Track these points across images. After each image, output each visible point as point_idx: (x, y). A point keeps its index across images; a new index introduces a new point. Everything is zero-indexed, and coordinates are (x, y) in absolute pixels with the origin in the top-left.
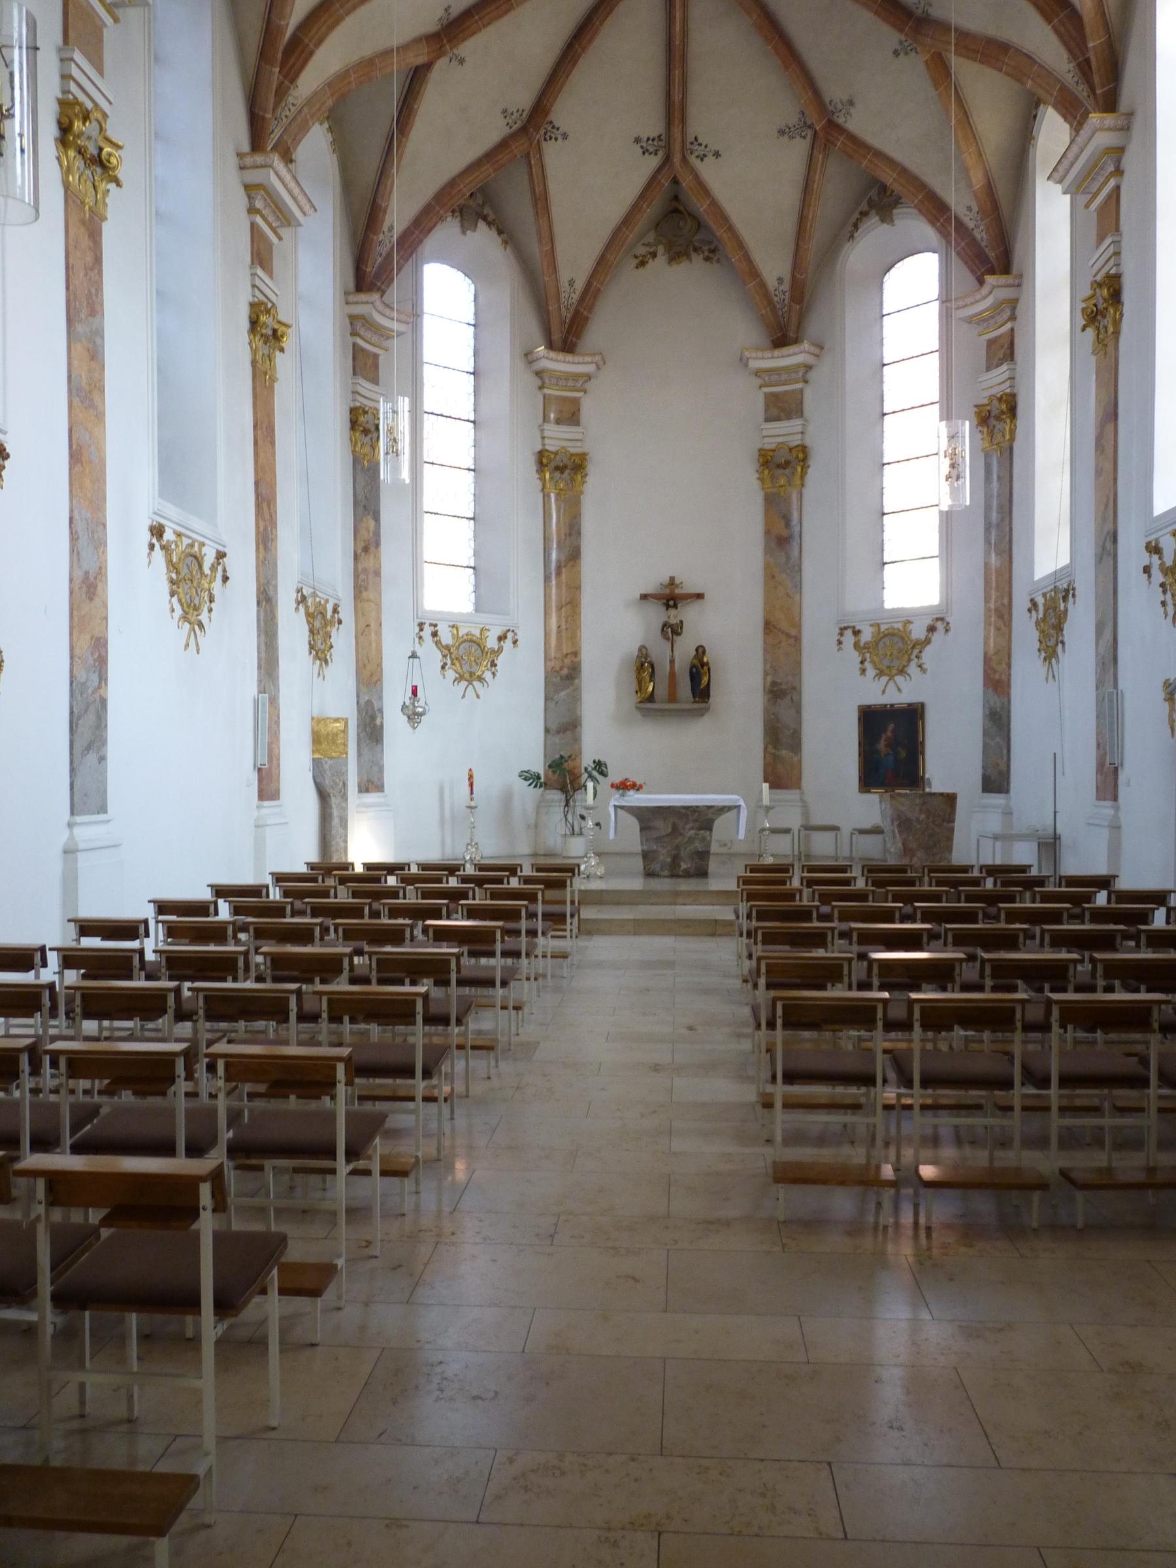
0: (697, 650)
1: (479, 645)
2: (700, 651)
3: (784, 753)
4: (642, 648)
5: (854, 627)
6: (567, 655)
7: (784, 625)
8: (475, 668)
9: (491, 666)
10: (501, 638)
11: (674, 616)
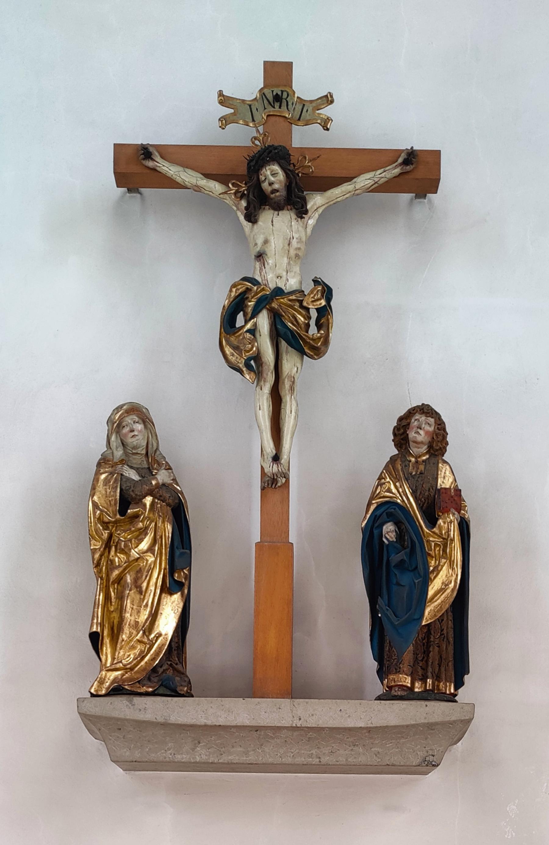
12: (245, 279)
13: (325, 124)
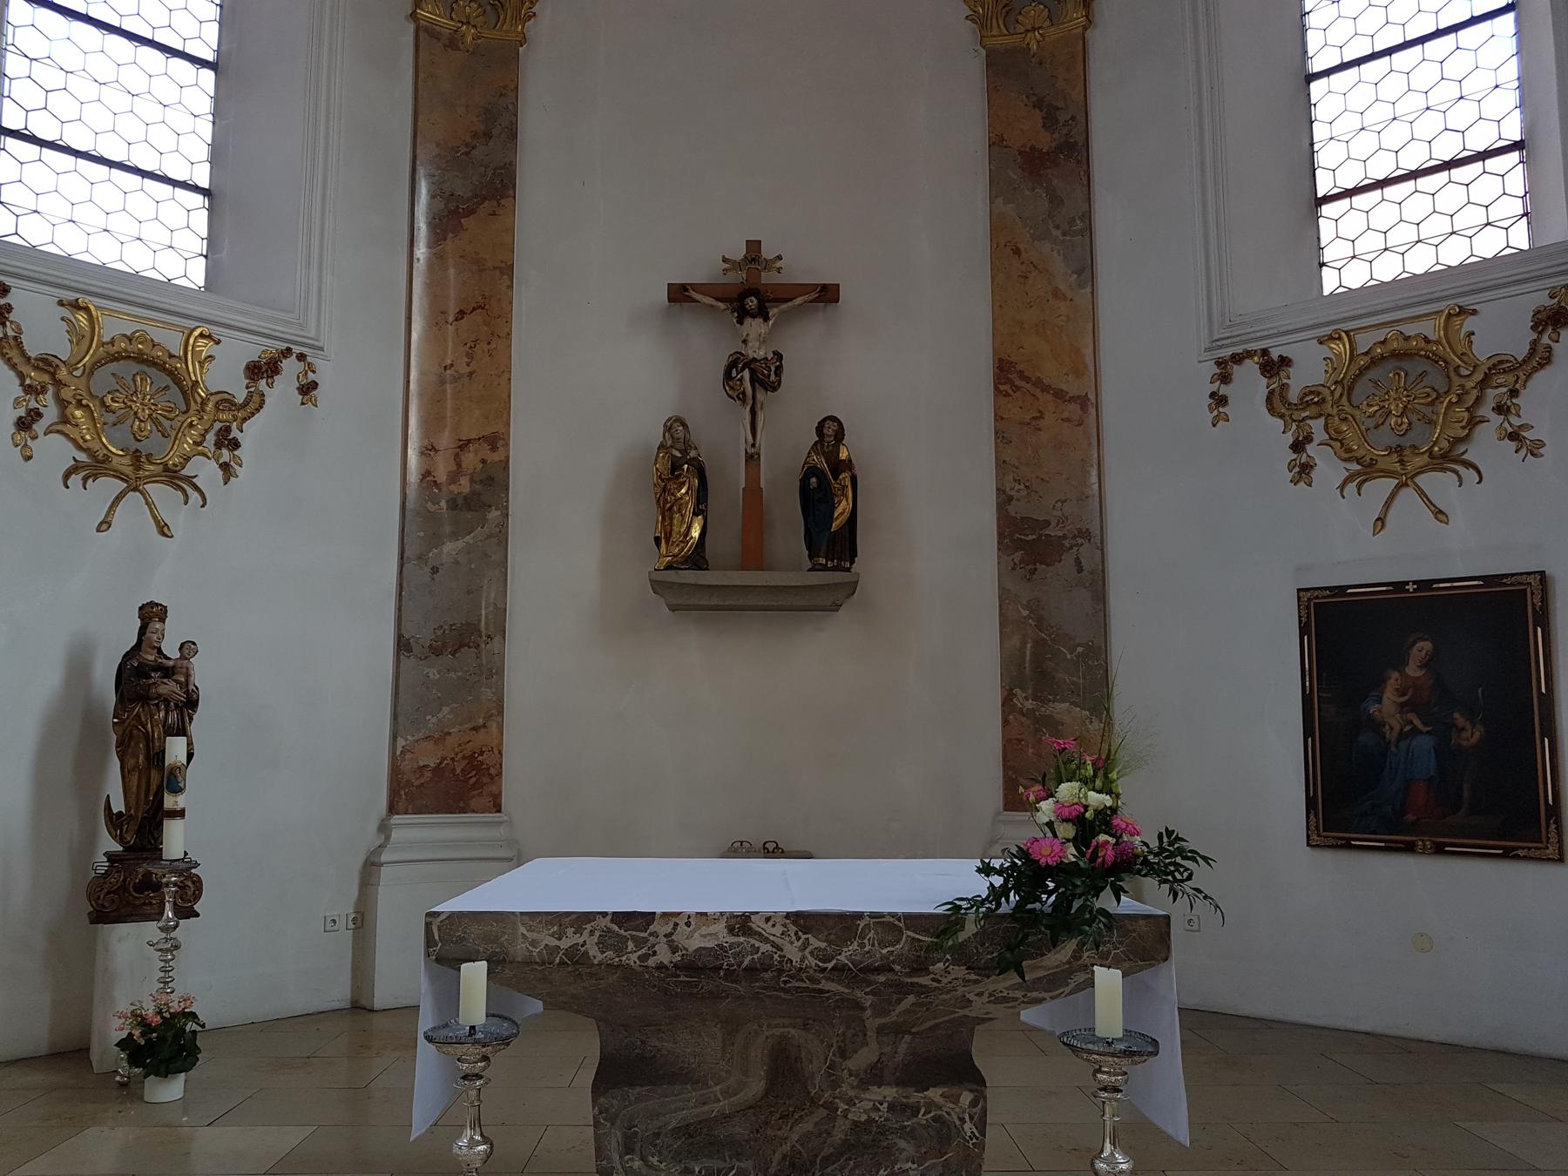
0: (820, 429)
1: (178, 381)
2: (830, 429)
3: (1060, 709)
4: (676, 425)
5: (1265, 352)
6: (469, 441)
7: (1051, 372)
8: (152, 443)
9: (219, 445)
10: (264, 370)
11: (756, 337)
12: (736, 353)
13: (779, 270)
